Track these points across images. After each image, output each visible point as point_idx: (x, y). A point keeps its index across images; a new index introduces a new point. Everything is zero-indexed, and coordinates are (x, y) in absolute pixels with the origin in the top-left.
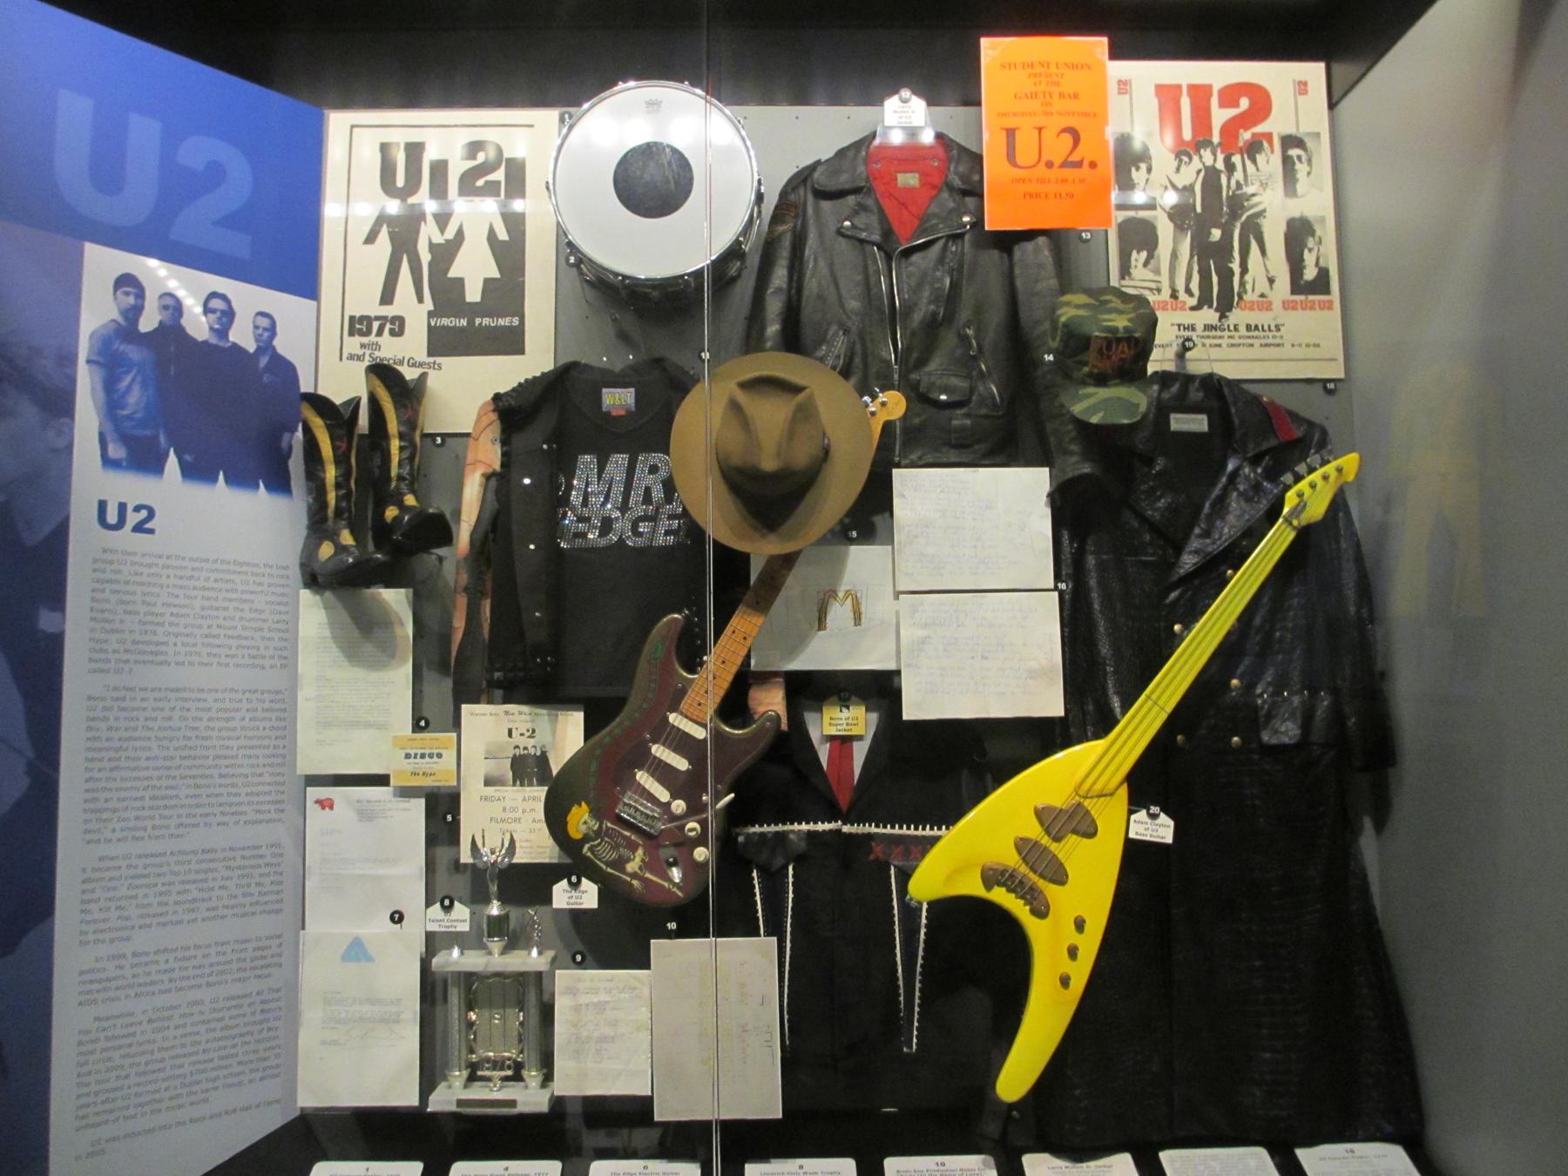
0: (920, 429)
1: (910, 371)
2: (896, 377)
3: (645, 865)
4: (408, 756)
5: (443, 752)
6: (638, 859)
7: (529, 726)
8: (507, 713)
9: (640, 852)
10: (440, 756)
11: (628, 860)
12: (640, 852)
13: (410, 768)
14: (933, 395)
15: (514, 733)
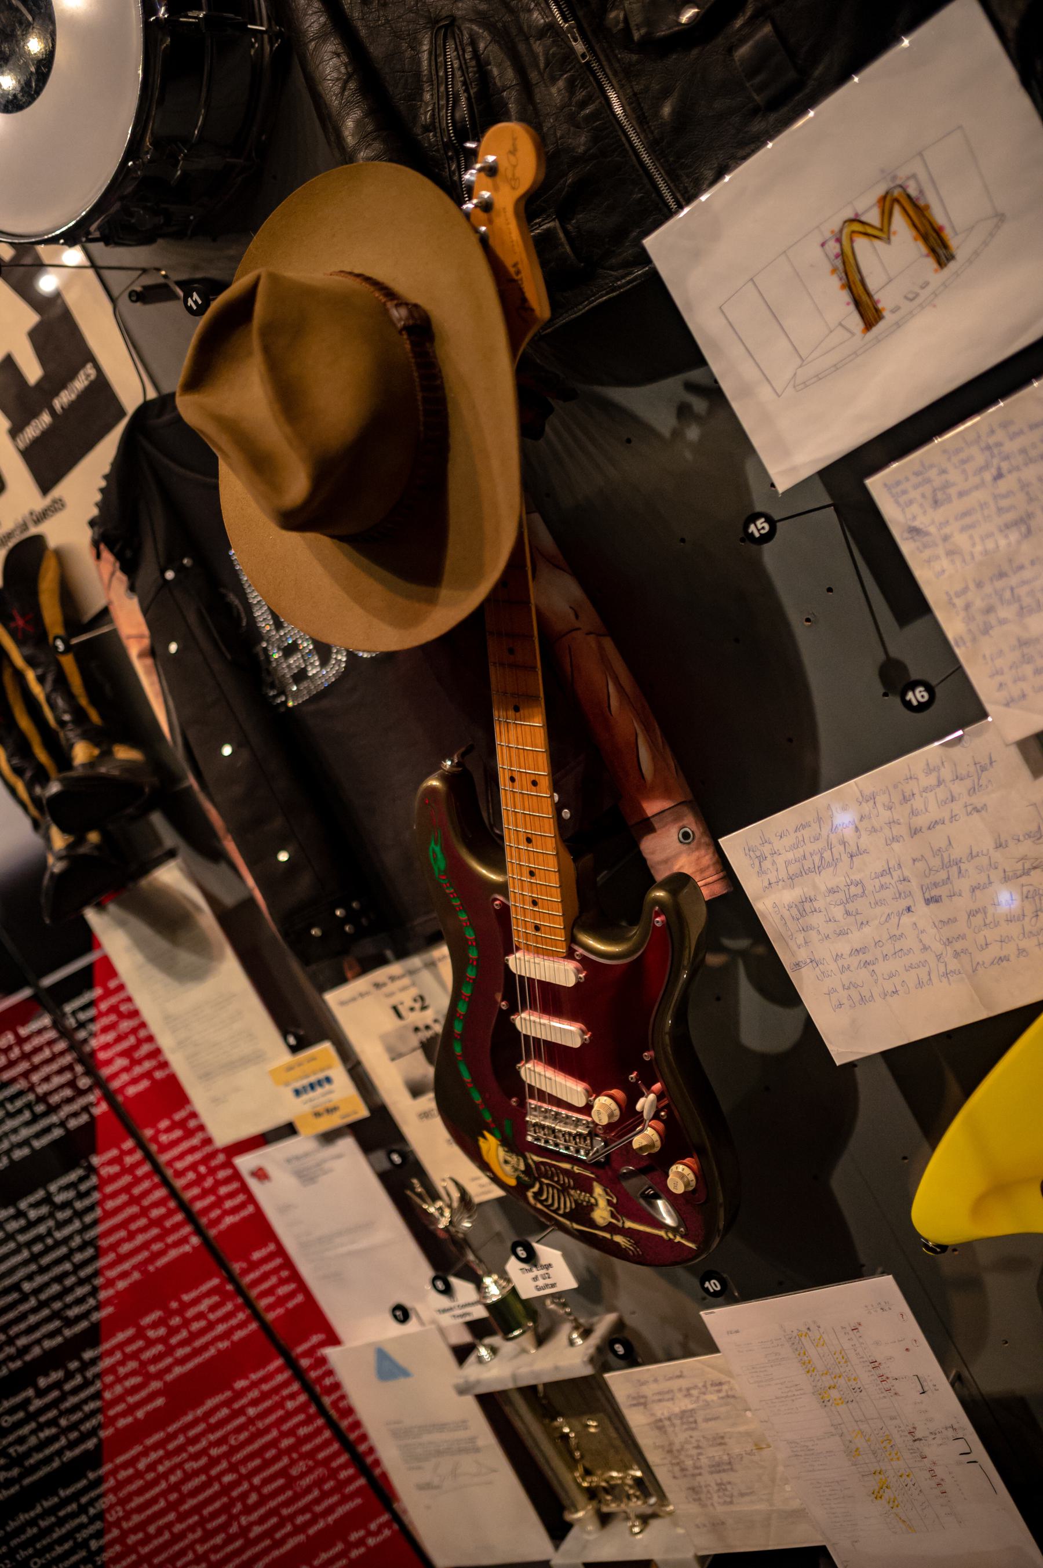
0: (682, 120)
1: (604, 11)
2: (579, 47)
3: (620, 1209)
4: (297, 1093)
5: (330, 1073)
6: (602, 1203)
7: (413, 992)
8: (377, 986)
9: (598, 1190)
10: (328, 1080)
11: (591, 1207)
12: (598, 1190)
13: (307, 1108)
14: (662, 32)
15: (402, 1010)
